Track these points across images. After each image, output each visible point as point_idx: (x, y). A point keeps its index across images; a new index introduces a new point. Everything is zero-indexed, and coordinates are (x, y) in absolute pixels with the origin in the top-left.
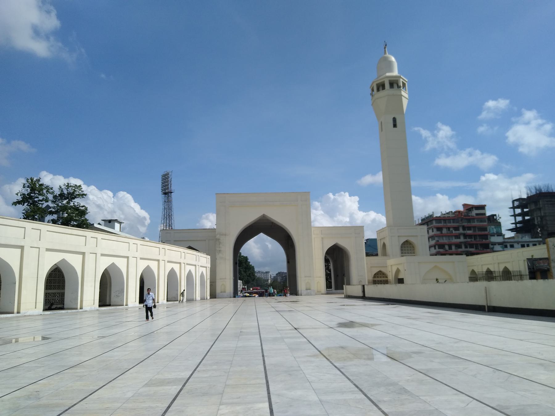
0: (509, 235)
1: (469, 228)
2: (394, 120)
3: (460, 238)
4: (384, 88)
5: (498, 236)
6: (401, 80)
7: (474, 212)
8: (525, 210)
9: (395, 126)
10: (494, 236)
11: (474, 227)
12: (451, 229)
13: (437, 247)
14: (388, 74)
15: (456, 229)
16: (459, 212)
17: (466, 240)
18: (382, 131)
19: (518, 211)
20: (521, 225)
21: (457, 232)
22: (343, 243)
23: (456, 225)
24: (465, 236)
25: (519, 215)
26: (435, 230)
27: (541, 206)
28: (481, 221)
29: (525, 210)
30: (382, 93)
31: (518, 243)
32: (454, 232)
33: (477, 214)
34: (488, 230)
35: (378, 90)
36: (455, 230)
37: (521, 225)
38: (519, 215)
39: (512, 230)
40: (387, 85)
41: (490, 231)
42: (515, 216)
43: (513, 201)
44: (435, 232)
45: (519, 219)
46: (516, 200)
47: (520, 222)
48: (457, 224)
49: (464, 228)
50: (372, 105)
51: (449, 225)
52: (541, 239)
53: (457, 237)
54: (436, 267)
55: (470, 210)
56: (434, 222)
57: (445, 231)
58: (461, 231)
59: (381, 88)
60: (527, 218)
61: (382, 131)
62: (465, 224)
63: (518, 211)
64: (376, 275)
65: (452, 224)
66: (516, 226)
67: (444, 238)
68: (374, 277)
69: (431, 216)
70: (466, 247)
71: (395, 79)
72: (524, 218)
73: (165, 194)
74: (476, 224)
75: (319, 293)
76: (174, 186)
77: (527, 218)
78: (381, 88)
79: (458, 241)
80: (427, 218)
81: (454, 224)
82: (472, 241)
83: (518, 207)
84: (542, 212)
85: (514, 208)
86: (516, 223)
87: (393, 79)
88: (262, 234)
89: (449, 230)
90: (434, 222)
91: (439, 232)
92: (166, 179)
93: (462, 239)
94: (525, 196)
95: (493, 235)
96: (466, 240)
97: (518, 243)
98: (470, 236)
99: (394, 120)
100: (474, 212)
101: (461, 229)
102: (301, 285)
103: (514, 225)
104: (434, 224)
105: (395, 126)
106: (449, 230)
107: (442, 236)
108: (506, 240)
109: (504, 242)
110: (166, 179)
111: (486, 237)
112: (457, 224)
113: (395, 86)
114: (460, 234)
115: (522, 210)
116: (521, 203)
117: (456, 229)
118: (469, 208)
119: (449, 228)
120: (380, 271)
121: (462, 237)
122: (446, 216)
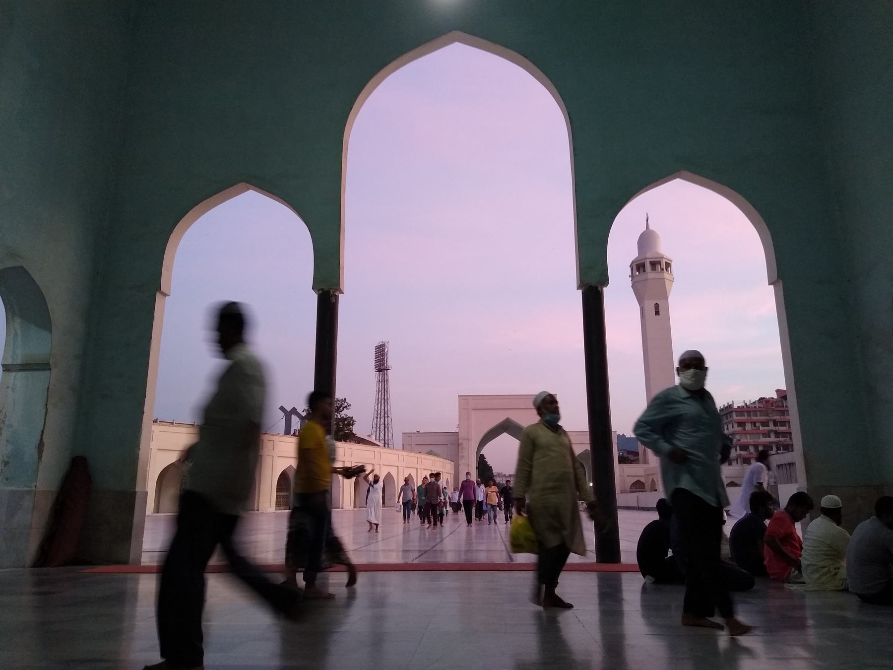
2: (657, 306)
4: (644, 271)
9: (657, 313)
12: (757, 425)
13: (738, 448)
14: (650, 255)
15: (765, 424)
21: (766, 428)
23: (763, 418)
24: (777, 434)
26: (735, 425)
32: (761, 428)
36: (763, 426)
40: (648, 267)
44: (737, 428)
49: (775, 423)
51: (754, 418)
53: (767, 434)
56: (734, 414)
57: (748, 427)
58: (772, 427)
59: (642, 270)
67: (748, 436)
69: (730, 406)
73: (379, 371)
78: (642, 270)
79: (767, 440)
80: (726, 408)
90: (734, 414)
91: (740, 429)
92: (381, 352)
93: (773, 438)
99: (657, 306)
104: (735, 417)
105: (657, 313)
107: (745, 433)
110: (381, 352)
114: (770, 431)
117: (765, 424)
119: (754, 424)
121: (772, 435)
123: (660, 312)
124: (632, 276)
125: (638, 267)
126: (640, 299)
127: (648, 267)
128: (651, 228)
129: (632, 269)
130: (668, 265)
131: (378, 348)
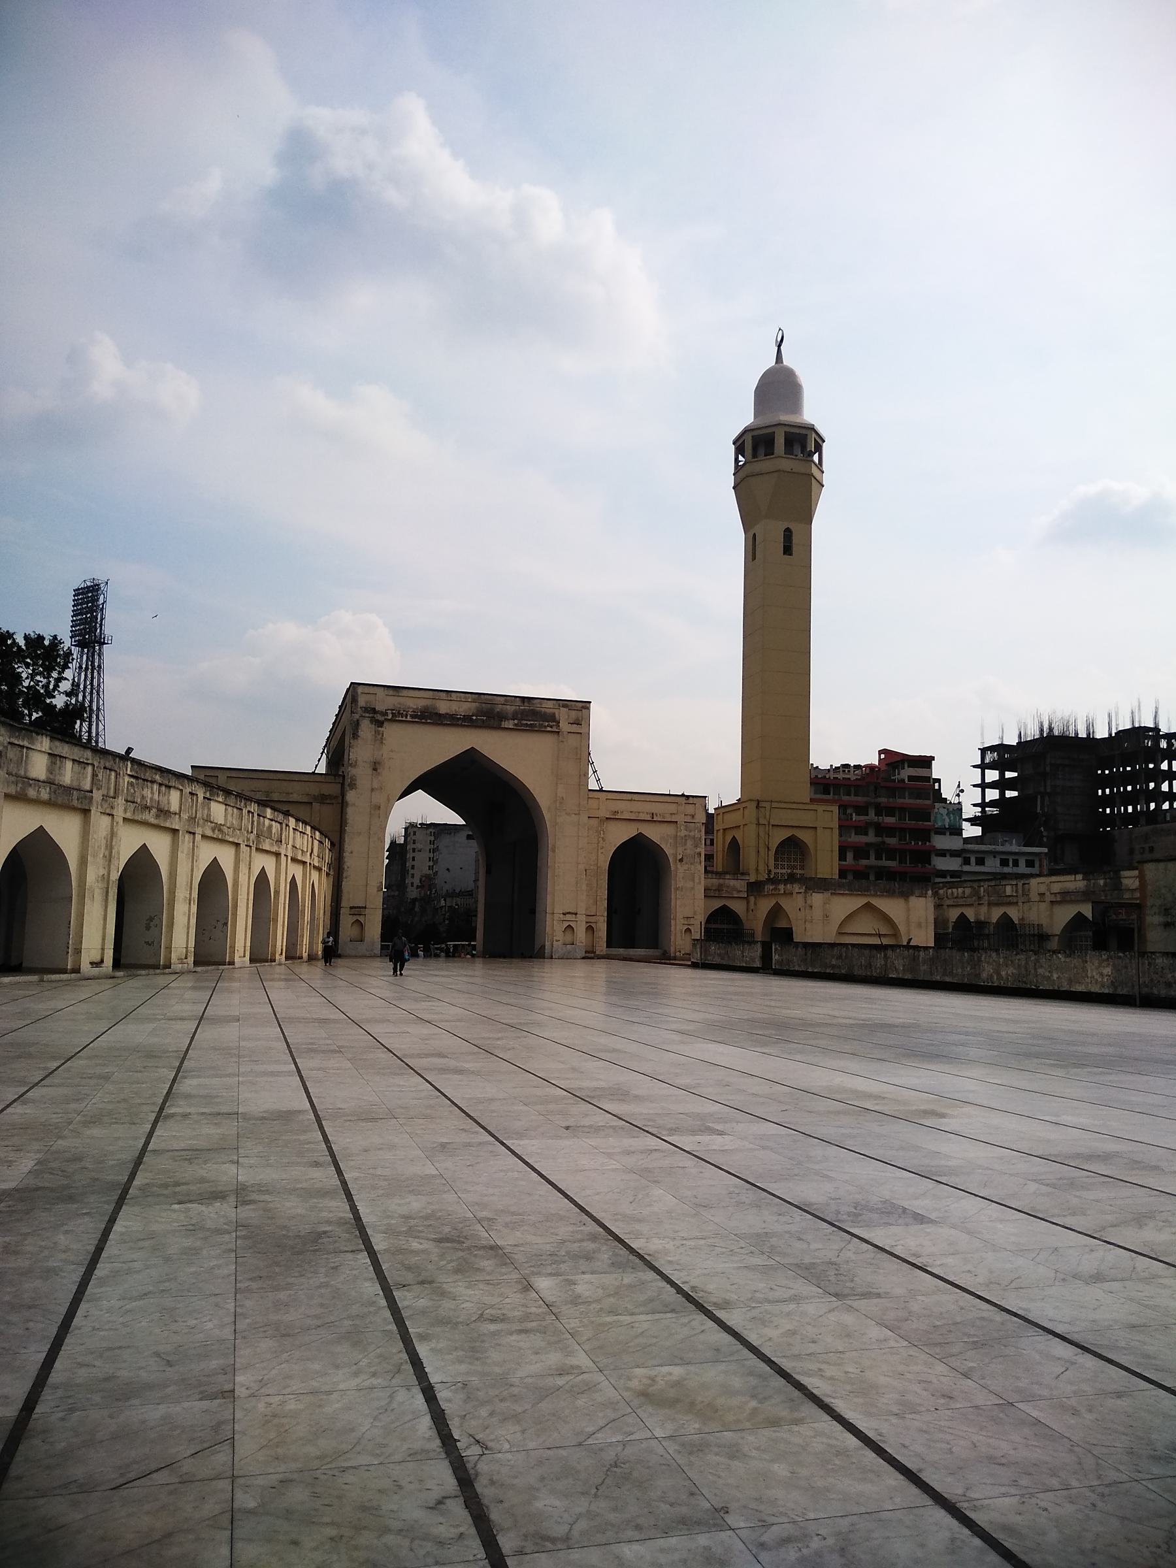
0: (971, 831)
1: (890, 811)
2: (788, 533)
3: (866, 834)
5: (951, 834)
6: (814, 435)
7: (907, 772)
8: (1009, 775)
9: (788, 550)
10: (944, 834)
11: (902, 810)
12: (849, 811)
15: (861, 810)
16: (871, 767)
17: (879, 839)
18: (754, 558)
19: (992, 775)
20: (995, 811)
21: (862, 818)
22: (654, 833)
24: (880, 830)
25: (993, 785)
27: (1048, 769)
28: (919, 797)
29: (1009, 775)
30: (766, 465)
31: (994, 854)
33: (911, 778)
34: (932, 818)
35: (755, 455)
37: (995, 811)
38: (993, 785)
39: (973, 821)
40: (780, 442)
41: (935, 821)
42: (983, 786)
43: (983, 751)
45: (992, 794)
46: (992, 749)
47: (993, 803)
48: (865, 799)
52: (1046, 850)
54: (868, 906)
55: (897, 767)
58: (872, 816)
59: (761, 451)
60: (1010, 794)
61: (754, 558)
62: (883, 800)
63: (992, 775)
64: (713, 917)
65: (853, 798)
66: (983, 811)
68: (708, 921)
70: (878, 858)
72: (1002, 794)
74: (908, 801)
75: (590, 955)
76: (113, 622)
77: (1010, 794)
78: (761, 451)
79: (864, 839)
81: (859, 799)
82: (892, 841)
83: (992, 766)
84: (1048, 783)
85: (983, 767)
86: (983, 805)
88: (420, 793)
89: (845, 813)
93: (871, 838)
94: (1012, 741)
95: (941, 831)
96: (879, 839)
97: (994, 854)
98: (890, 831)
99: (788, 533)
100: (907, 772)
101: (872, 813)
102: (553, 929)
103: (980, 809)
105: (788, 550)
106: (845, 813)
108: (969, 847)
109: (964, 850)
111: (925, 834)
112: (865, 799)
113: (797, 449)
115: (1002, 775)
116: (999, 756)
118: (893, 760)
120: (724, 907)
121: (871, 832)
122: (840, 776)
123: (795, 549)
125: (755, 445)
127: (780, 442)
128: (787, 361)
130: (819, 448)
131: (78, 592)
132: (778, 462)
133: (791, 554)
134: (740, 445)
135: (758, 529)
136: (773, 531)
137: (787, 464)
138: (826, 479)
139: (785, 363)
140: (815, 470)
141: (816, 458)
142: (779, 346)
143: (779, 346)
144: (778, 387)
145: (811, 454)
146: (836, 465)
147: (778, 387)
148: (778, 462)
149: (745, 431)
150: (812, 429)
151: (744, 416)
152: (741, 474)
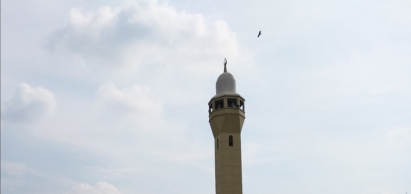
2: (231, 138)
4: (222, 106)
6: (240, 99)
9: (231, 144)
18: (218, 148)
30: (220, 112)
35: (216, 108)
40: (226, 103)
50: (209, 122)
59: (219, 106)
61: (218, 148)
71: (233, 98)
78: (219, 106)
87: (230, 98)
99: (231, 138)
105: (231, 144)
123: (234, 144)
124: (210, 111)
126: (216, 132)
127: (226, 103)
129: (211, 107)
130: (242, 103)
132: (226, 110)
133: (232, 146)
134: (210, 105)
135: (219, 137)
136: (225, 137)
137: (229, 111)
138: (246, 115)
139: (228, 72)
140: (241, 113)
141: (241, 108)
142: (225, 65)
143: (225, 65)
144: (225, 81)
145: (238, 107)
146: (249, 109)
147: (225, 81)
148: (226, 110)
149: (212, 99)
150: (239, 96)
151: (212, 93)
152: (211, 116)
